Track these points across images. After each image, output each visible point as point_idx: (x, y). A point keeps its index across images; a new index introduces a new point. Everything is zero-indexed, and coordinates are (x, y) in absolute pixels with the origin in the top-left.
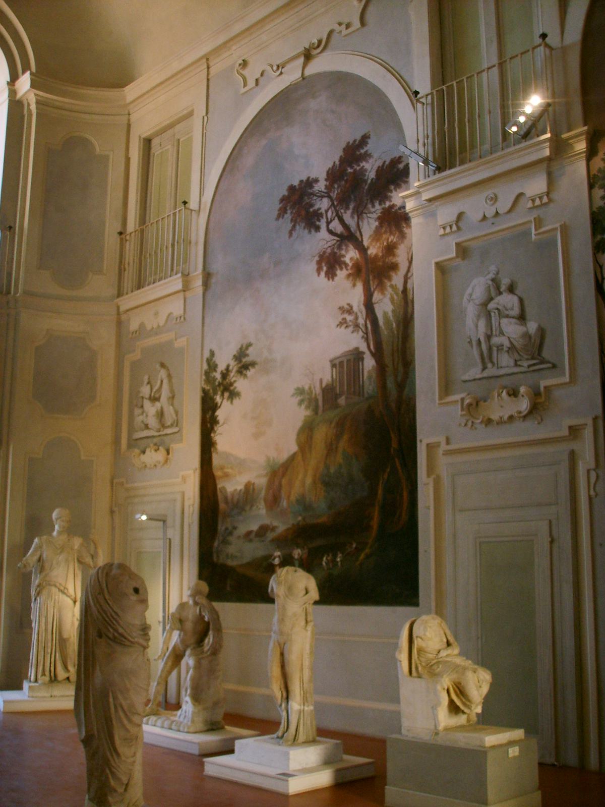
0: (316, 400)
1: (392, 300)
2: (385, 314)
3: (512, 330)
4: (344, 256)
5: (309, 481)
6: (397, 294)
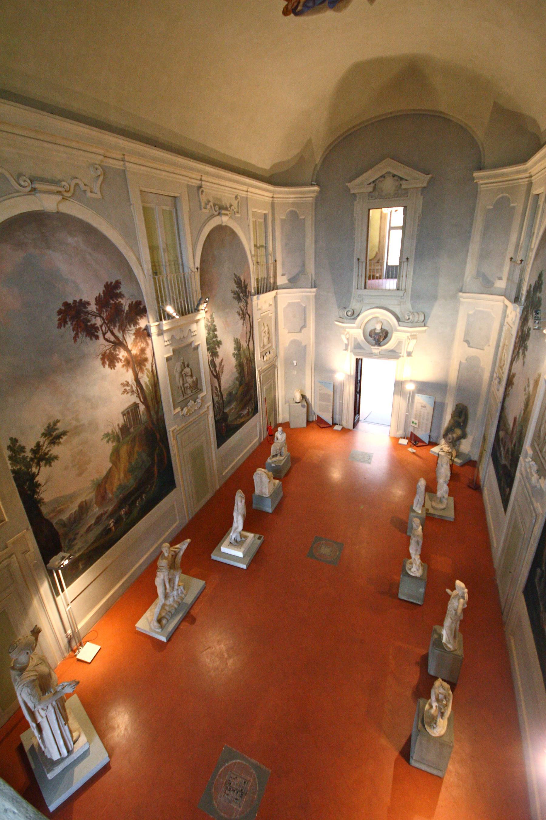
0: (118, 436)
1: (148, 376)
2: (146, 383)
3: (190, 380)
4: (118, 355)
5: (122, 475)
6: (149, 372)
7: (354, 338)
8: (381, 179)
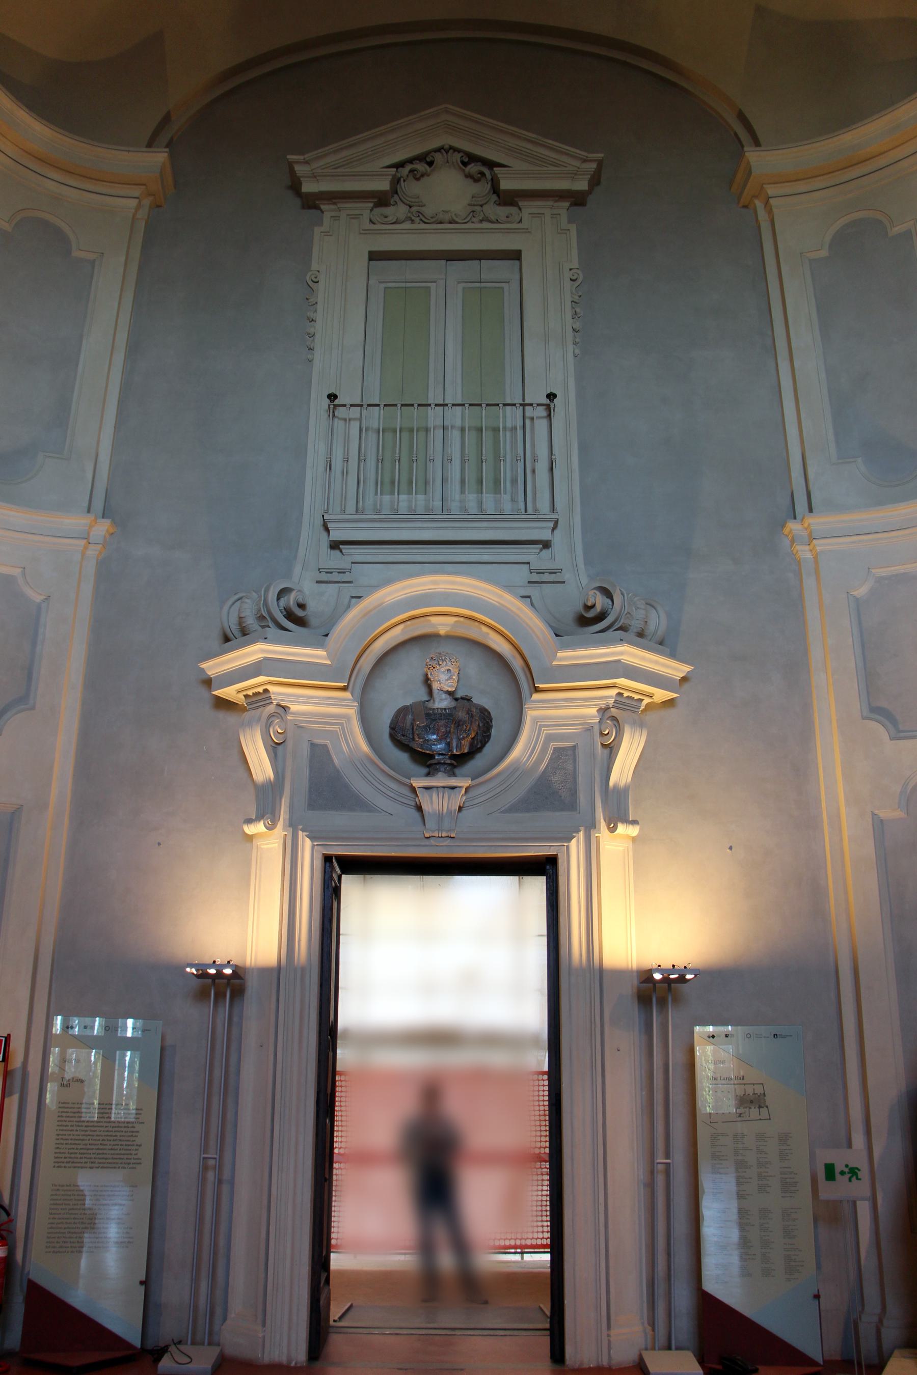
7: (313, 745)
8: (421, 167)
